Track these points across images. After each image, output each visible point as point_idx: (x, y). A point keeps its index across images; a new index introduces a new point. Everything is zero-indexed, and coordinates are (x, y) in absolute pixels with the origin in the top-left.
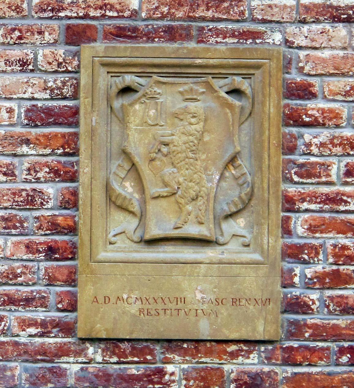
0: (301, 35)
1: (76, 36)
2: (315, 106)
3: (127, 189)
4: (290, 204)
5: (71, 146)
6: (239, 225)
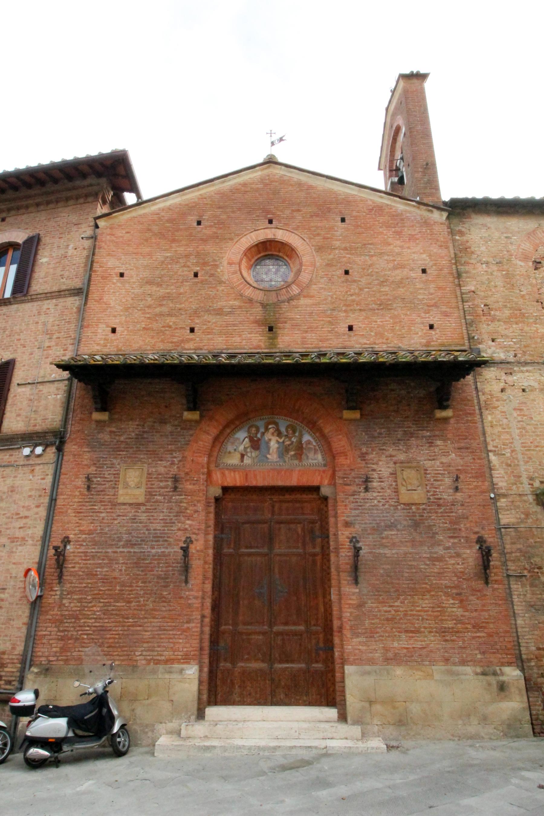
0: (425, 462)
1: (395, 463)
2: (428, 472)
3: (404, 483)
4: (426, 485)
5: (396, 478)
6: (420, 488)
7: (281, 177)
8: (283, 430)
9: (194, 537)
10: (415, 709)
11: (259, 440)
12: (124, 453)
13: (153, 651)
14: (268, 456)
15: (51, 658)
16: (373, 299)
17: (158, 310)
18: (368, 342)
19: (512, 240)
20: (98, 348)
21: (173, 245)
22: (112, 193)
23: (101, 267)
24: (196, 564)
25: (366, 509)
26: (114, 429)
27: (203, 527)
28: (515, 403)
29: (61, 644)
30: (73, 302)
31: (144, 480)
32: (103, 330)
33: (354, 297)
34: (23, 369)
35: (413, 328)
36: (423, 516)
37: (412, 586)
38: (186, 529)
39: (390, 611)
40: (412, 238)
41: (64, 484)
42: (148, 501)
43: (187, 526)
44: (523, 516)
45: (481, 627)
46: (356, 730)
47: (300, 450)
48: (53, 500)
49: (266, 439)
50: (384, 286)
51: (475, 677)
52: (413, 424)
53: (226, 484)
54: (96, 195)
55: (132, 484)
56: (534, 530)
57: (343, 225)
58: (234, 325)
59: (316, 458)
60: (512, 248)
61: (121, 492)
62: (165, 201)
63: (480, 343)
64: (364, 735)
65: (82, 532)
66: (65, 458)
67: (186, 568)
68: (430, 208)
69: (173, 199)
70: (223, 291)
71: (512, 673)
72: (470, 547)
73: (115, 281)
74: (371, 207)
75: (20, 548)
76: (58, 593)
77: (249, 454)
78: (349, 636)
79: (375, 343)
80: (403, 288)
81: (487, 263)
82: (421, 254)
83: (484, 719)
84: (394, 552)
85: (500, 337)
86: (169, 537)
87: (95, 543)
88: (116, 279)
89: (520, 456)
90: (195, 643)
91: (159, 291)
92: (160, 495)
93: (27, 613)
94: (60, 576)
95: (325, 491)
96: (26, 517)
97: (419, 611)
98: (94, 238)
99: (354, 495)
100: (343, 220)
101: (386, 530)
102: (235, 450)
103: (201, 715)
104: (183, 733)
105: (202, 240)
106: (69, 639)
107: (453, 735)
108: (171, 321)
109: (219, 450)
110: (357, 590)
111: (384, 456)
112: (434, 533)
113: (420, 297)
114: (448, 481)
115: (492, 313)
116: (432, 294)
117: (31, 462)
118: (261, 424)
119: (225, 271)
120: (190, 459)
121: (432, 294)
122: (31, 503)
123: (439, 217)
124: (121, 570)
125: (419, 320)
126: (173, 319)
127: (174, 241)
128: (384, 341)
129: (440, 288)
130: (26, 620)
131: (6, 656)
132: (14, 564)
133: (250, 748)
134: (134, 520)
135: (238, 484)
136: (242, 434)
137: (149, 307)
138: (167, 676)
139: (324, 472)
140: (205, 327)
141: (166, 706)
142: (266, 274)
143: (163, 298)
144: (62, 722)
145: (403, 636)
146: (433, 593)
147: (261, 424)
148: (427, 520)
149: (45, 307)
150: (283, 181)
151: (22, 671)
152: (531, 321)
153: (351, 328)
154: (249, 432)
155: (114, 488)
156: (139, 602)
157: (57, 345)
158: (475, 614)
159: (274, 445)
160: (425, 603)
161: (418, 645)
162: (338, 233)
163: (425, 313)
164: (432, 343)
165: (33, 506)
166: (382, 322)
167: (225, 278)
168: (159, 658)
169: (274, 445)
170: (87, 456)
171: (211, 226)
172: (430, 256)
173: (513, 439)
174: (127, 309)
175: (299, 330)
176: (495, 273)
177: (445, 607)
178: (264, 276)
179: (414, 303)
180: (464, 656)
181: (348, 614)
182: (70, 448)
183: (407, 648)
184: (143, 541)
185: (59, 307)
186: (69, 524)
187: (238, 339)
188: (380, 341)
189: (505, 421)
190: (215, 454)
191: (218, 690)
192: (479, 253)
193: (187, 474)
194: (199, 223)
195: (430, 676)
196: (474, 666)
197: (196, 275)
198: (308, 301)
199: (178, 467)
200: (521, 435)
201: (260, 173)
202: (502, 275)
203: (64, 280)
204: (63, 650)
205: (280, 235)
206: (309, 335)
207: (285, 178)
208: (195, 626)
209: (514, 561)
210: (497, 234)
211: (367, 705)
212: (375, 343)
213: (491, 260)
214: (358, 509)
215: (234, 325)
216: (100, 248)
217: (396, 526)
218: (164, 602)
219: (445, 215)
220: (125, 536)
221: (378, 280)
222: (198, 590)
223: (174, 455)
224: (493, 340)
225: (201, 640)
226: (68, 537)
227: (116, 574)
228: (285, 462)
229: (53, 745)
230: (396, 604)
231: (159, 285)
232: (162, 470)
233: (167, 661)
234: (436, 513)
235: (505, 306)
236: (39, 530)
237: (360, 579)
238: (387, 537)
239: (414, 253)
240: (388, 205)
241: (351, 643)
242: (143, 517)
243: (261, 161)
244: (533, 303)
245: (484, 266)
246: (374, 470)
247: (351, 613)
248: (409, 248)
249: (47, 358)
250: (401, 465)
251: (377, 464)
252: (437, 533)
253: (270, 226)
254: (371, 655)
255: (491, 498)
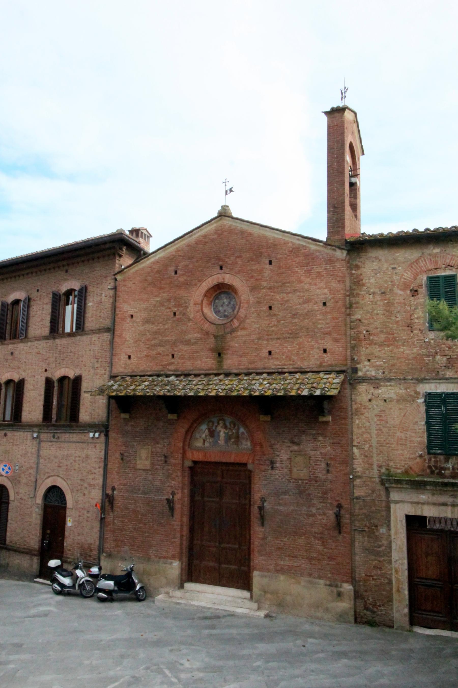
1: (291, 452)
2: (311, 458)
4: (309, 467)
5: (291, 461)
6: (305, 469)
7: (230, 227)
8: (228, 424)
9: (176, 491)
10: (288, 598)
11: (214, 431)
12: (139, 439)
13: (158, 551)
14: (219, 442)
15: (111, 550)
16: (286, 329)
17: (153, 342)
18: (281, 364)
19: (397, 271)
20: (121, 370)
21: (160, 291)
22: (125, 247)
23: (120, 311)
24: (177, 506)
25: (271, 481)
26: (133, 423)
27: (181, 485)
28: (377, 411)
29: (115, 543)
30: (106, 336)
31: (150, 455)
32: (124, 357)
33: (273, 328)
34: (86, 381)
35: (311, 352)
36: (305, 488)
37: (295, 530)
38: (172, 486)
39: (280, 544)
40: (319, 275)
41: (110, 456)
42: (152, 468)
43: (172, 485)
44: (370, 492)
45: (333, 559)
46: (255, 605)
47: (238, 439)
48: (106, 466)
49: (218, 430)
50: (295, 318)
51: (324, 587)
52: (305, 425)
53: (194, 460)
54: (114, 255)
55: (143, 458)
56: (376, 501)
57: (271, 267)
58: (197, 352)
59: (246, 444)
60: (396, 278)
61: (138, 462)
62: (154, 256)
63: (358, 363)
64: (259, 609)
65: (120, 484)
66: (110, 441)
67: (172, 509)
68: (334, 248)
69: (159, 253)
70: (191, 326)
71: (347, 587)
72: (332, 510)
73: (128, 321)
74: (291, 249)
75: (93, 490)
76: (112, 516)
77: (208, 440)
78: (257, 555)
79: (285, 365)
80: (308, 319)
81: (374, 293)
82: (324, 289)
83: (327, 610)
84: (286, 508)
85: (374, 358)
86: (163, 490)
87: (127, 491)
88: (129, 319)
89: (375, 450)
90: (178, 550)
91: (153, 328)
92: (159, 465)
93: (99, 526)
94: (112, 508)
95: (250, 467)
96: (95, 473)
97: (297, 545)
98: (115, 288)
99: (265, 471)
100: (270, 263)
101: (282, 495)
102: (200, 437)
103: (181, 586)
104: (171, 594)
105: (177, 286)
106: (119, 541)
107: (308, 616)
108: (160, 349)
109: (191, 437)
110: (263, 530)
111: (285, 446)
112: (311, 499)
113: (319, 326)
114: (323, 465)
115: (371, 338)
116: (327, 324)
117: (94, 441)
118: (215, 420)
119: (192, 310)
120: (173, 444)
121: (327, 324)
122: (97, 466)
123: (341, 254)
124: (140, 507)
125: (316, 346)
126: (162, 349)
127: (161, 288)
128: (291, 363)
129: (334, 318)
130: (99, 529)
131: (92, 546)
132: (91, 498)
133: (197, 606)
134: (145, 479)
135: (201, 460)
136: (204, 427)
137: (148, 340)
138: (164, 565)
139: (250, 454)
140: (180, 354)
141: (164, 581)
142: (222, 306)
143: (156, 333)
144: (112, 583)
145: (287, 559)
146: (306, 536)
147: (215, 420)
148: (307, 490)
149: (93, 339)
150: (231, 231)
151: (99, 553)
152: (400, 344)
153: (270, 353)
154: (208, 426)
155: (135, 460)
156: (150, 525)
157: (101, 367)
158: (330, 551)
159: (222, 434)
160: (301, 541)
161: (295, 564)
162: (266, 274)
163: (322, 340)
164: (324, 364)
165: (97, 467)
166: (290, 347)
167: (192, 316)
168: (161, 555)
169: (222, 434)
170: (120, 440)
171: (183, 275)
172: (330, 290)
173: (371, 437)
174: (136, 342)
175: (237, 355)
176: (379, 303)
177: (313, 545)
178: (221, 309)
179: (314, 332)
180: (321, 574)
181: (257, 543)
182: (112, 434)
183: (289, 566)
184: (150, 491)
185: (101, 340)
186: (115, 480)
187: (199, 362)
188: (289, 363)
189: (368, 424)
190: (188, 440)
191: (192, 574)
192: (368, 285)
193: (172, 453)
194: (176, 272)
195: (299, 583)
196: (326, 580)
197: (175, 314)
198: (244, 333)
199: (167, 449)
200: (378, 435)
201: (215, 225)
202: (384, 304)
203: (101, 320)
204: (117, 546)
205: (228, 278)
206: (243, 359)
207: (233, 227)
208: (177, 541)
209: (359, 521)
210: (385, 266)
211: (263, 593)
212: (285, 365)
213: (377, 290)
214: (267, 481)
215: (197, 352)
216: (119, 297)
217: (288, 493)
218: (162, 526)
219: (345, 252)
220: (142, 488)
221: (291, 313)
222: (180, 521)
223: (165, 441)
224: (369, 360)
225: (181, 549)
226: (114, 487)
227: (138, 509)
228: (228, 446)
229: (109, 592)
230: (284, 540)
231: (153, 323)
232: (159, 450)
233: (165, 558)
234: (314, 486)
235: (382, 332)
236: (100, 481)
237: (265, 523)
238: (282, 499)
239: (318, 289)
240: (303, 246)
241: (257, 559)
242: (150, 478)
243: (216, 215)
244: (404, 328)
245: (371, 296)
246: (278, 456)
247: (259, 543)
248: (315, 284)
249: (97, 375)
250: (295, 453)
251: (280, 451)
252: (313, 499)
253: (220, 271)
254: (268, 567)
255: (351, 479)
